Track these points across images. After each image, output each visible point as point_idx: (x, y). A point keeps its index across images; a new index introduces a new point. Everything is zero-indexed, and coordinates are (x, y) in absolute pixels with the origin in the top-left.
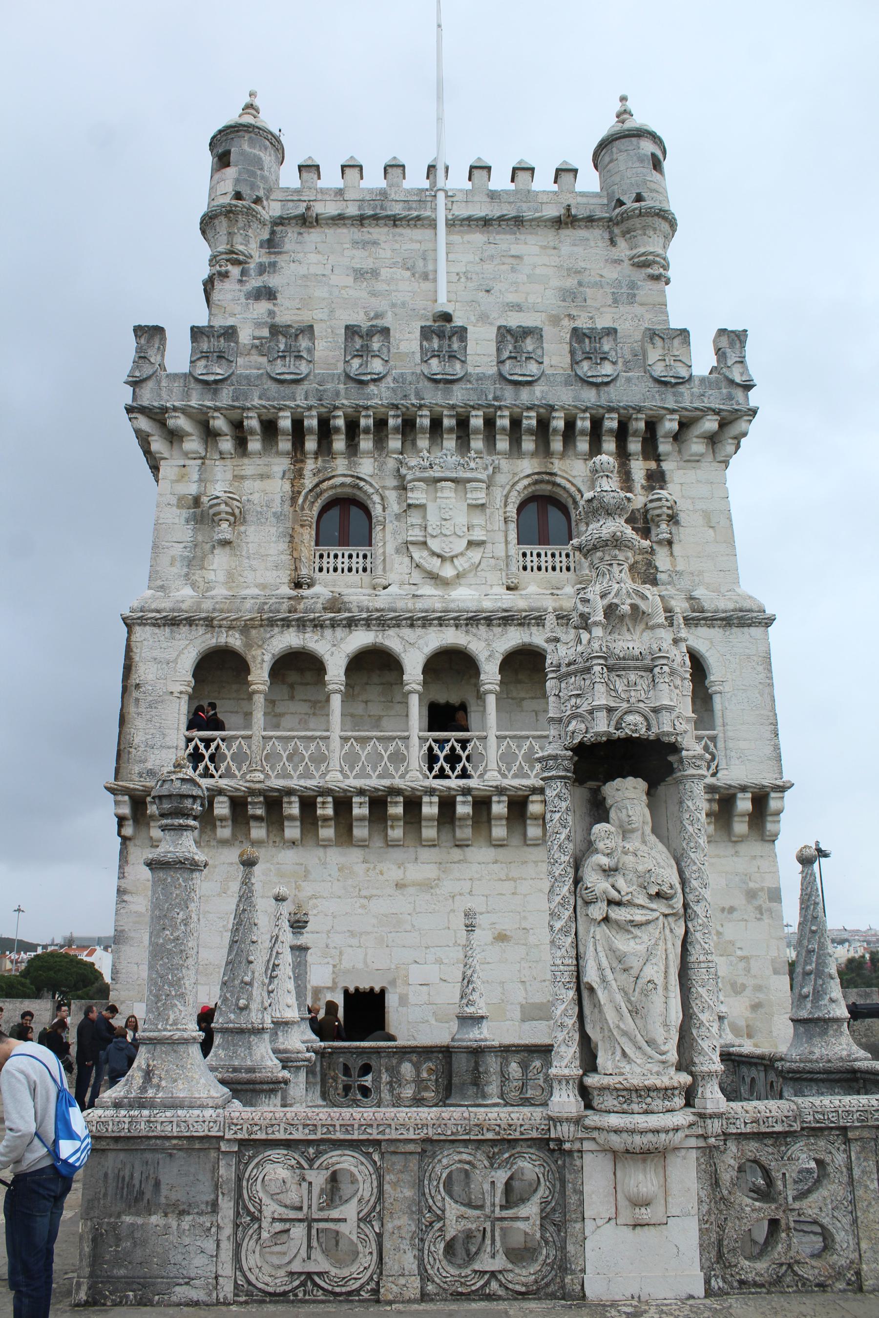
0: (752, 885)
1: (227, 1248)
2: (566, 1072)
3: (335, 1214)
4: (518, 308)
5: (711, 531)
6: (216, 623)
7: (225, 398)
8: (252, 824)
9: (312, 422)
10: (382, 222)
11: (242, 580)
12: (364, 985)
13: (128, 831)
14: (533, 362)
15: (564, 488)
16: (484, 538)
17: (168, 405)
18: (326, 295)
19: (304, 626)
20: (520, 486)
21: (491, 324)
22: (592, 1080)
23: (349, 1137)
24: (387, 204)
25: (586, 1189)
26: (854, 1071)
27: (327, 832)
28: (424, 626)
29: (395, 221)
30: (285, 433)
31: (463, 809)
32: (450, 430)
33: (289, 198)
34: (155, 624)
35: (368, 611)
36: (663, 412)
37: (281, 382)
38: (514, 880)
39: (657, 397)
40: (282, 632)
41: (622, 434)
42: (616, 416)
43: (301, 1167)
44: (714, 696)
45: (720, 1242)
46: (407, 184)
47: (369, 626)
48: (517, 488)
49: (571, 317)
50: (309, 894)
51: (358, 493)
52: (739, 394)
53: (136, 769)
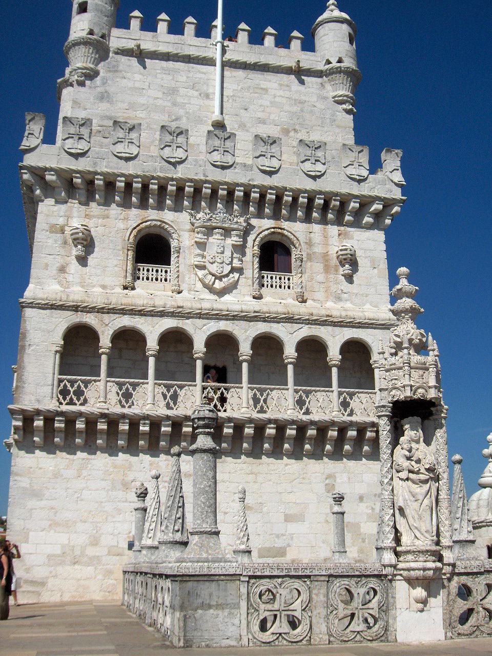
1: (244, 622)
2: (391, 545)
3: (291, 607)
5: (376, 271)
7: (82, 165)
9: (137, 186)
17: (47, 166)
18: (145, 102)
19: (135, 315)
20: (264, 233)
21: (247, 131)
22: (399, 549)
23: (297, 574)
25: (397, 596)
29: (188, 59)
33: (123, 36)
37: (121, 158)
43: (276, 588)
44: (375, 370)
45: (450, 618)
48: (261, 236)
50: (132, 479)
51: (162, 231)
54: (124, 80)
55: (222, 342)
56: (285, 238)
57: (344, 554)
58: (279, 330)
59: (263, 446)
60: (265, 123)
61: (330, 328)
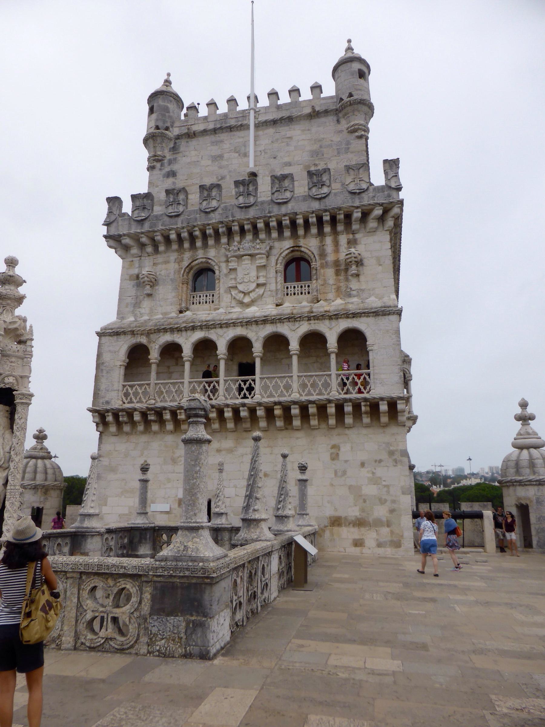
0: (392, 448)
4: (289, 164)
5: (380, 267)
6: (135, 332)
7: (147, 227)
8: (152, 424)
9: (185, 235)
10: (224, 130)
11: (156, 311)
13: (101, 429)
14: (288, 192)
15: (305, 253)
16: (265, 282)
17: (121, 233)
20: (284, 254)
24: (228, 120)
28: (227, 327)
29: (231, 129)
31: (244, 413)
33: (182, 125)
35: (202, 322)
36: (353, 208)
38: (272, 447)
39: (350, 201)
40: (164, 335)
42: (329, 213)
46: (239, 109)
47: (202, 329)
48: (282, 255)
49: (315, 165)
51: (209, 265)
52: (394, 193)
53: (101, 401)
54: (184, 158)
55: (240, 345)
56: (303, 254)
57: (305, 516)
58: (284, 329)
60: (290, 166)
61: (327, 322)
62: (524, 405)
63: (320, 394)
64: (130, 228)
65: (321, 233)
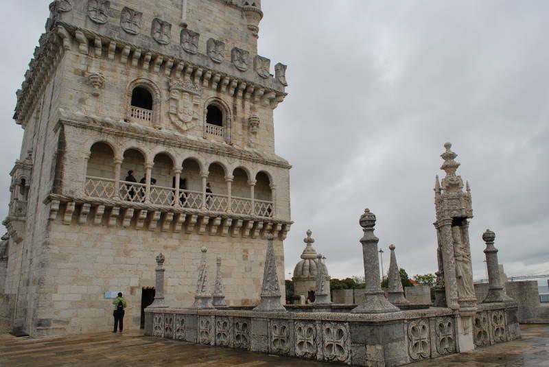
5: (267, 133)
9: (138, 54)
12: (151, 286)
15: (224, 106)
17: (78, 27)
26: (408, 306)
27: (140, 224)
28: (185, 148)
30: (125, 54)
31: (194, 220)
32: (189, 73)
34: (76, 126)
41: (245, 91)
47: (164, 144)
51: (151, 89)
52: (282, 87)
55: (191, 164)
58: (224, 161)
59: (244, 233)
61: (251, 163)
62: (309, 233)
63: (245, 213)
64: (86, 25)
65: (235, 96)
